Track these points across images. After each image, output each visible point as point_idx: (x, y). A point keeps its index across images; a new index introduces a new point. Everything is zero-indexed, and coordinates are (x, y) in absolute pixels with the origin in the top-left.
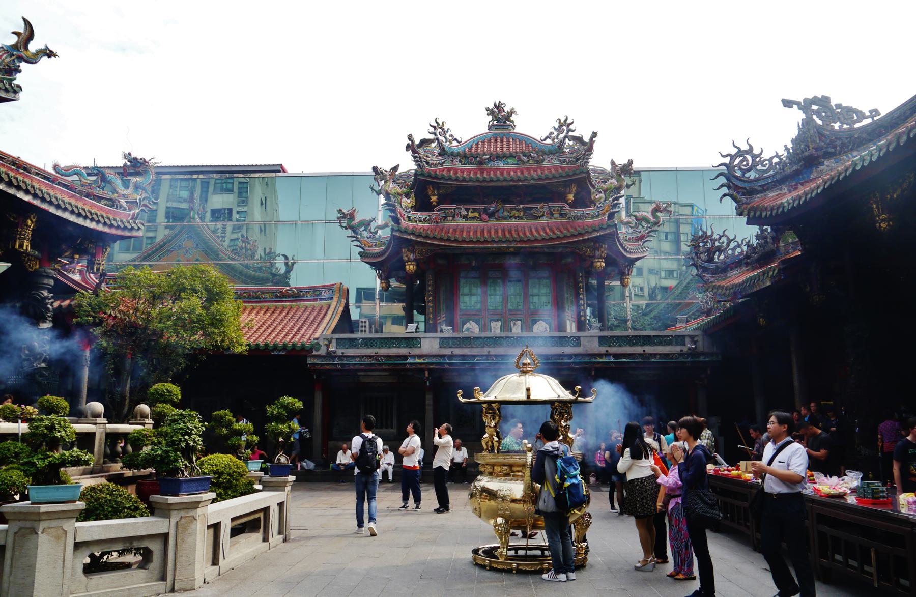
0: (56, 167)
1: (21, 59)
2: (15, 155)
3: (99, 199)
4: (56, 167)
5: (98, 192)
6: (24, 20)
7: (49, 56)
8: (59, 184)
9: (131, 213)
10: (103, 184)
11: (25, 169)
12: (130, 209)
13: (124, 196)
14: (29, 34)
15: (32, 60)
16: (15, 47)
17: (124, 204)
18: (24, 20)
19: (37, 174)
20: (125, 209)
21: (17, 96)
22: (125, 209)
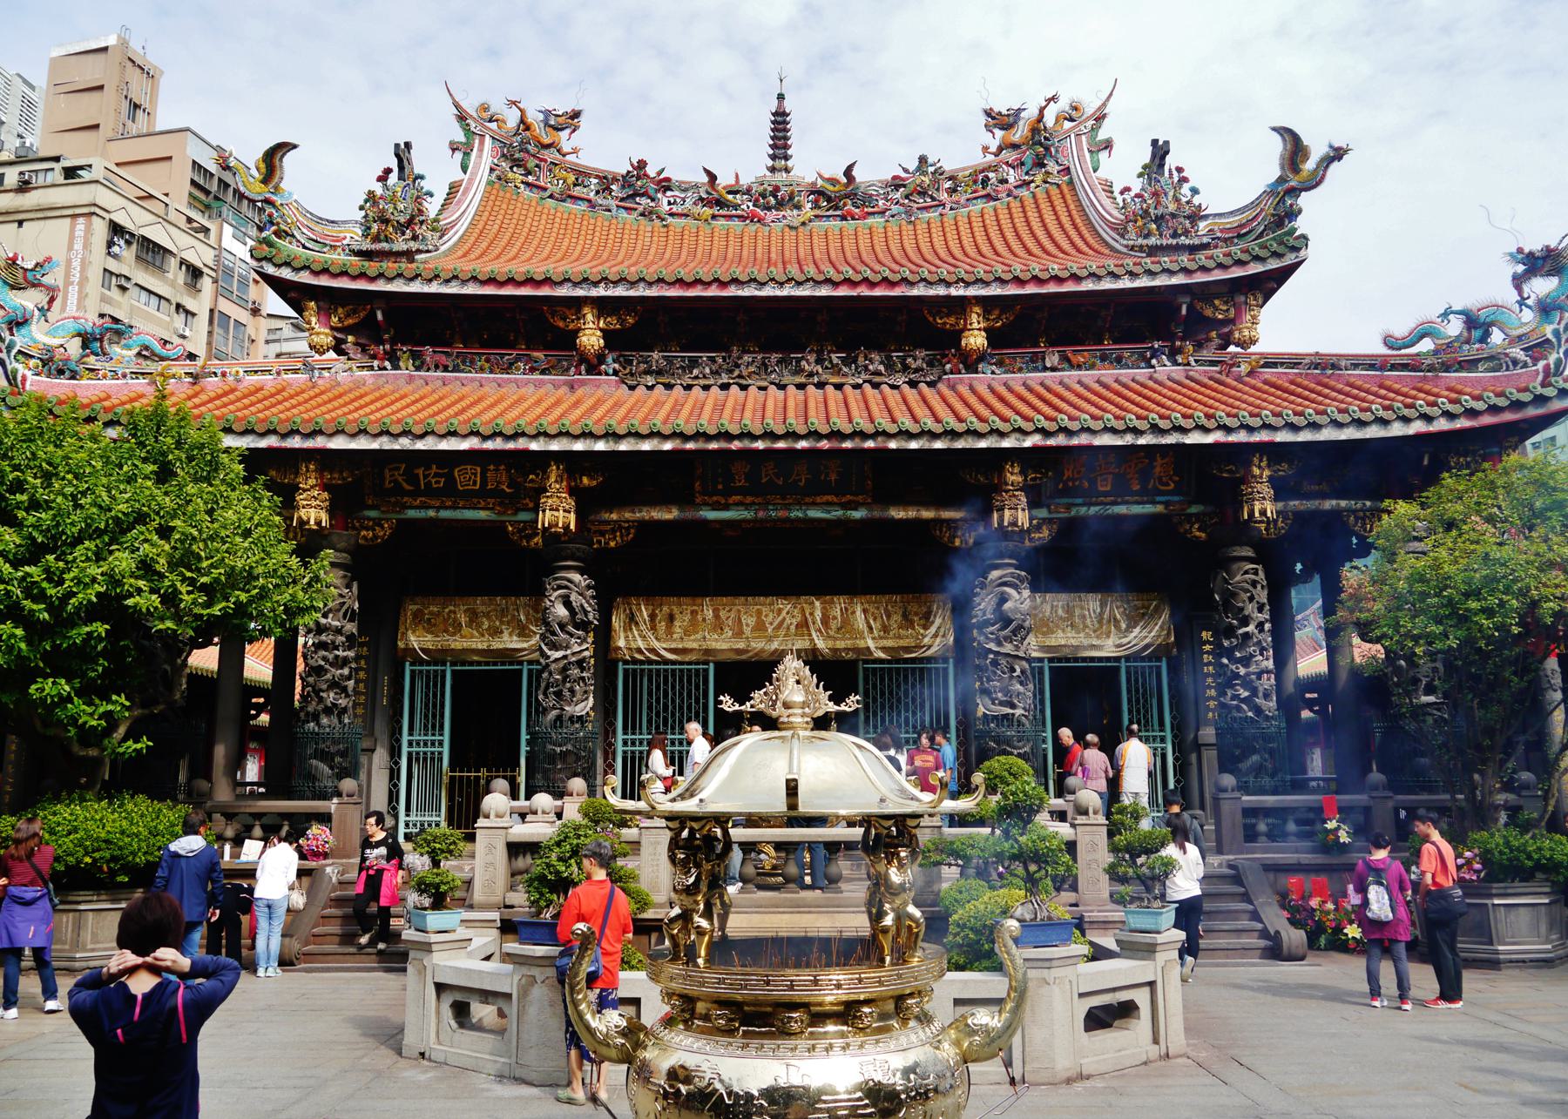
0: (1388, 341)
1: (1294, 192)
2: (1312, 350)
3: (1471, 364)
4: (1388, 341)
5: (1471, 351)
6: (1274, 129)
7: (1339, 158)
8: (1394, 367)
9: (1541, 364)
10: (1477, 334)
11: (1334, 366)
12: (1535, 361)
13: (1520, 337)
14: (1295, 149)
15: (1314, 182)
16: (1281, 180)
17: (1521, 356)
18: (1274, 129)
19: (1356, 366)
20: (1525, 365)
21: (1302, 253)
22: (1525, 365)
